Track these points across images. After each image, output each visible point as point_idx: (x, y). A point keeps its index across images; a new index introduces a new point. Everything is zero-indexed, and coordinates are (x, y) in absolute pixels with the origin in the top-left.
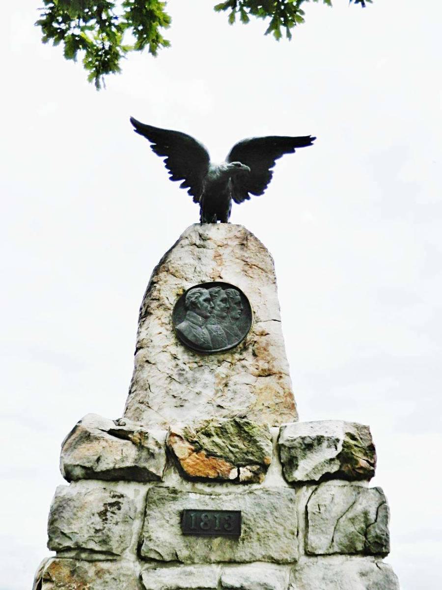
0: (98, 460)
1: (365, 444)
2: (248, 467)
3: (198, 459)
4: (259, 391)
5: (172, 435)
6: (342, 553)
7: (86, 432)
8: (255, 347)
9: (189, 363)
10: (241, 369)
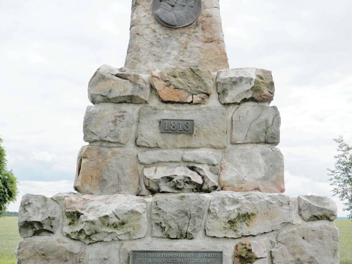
0: (110, 91)
1: (268, 82)
2: (198, 95)
3: (169, 90)
4: (205, 52)
5: (153, 76)
6: (251, 143)
7: (102, 75)
9: (163, 34)
10: (195, 38)
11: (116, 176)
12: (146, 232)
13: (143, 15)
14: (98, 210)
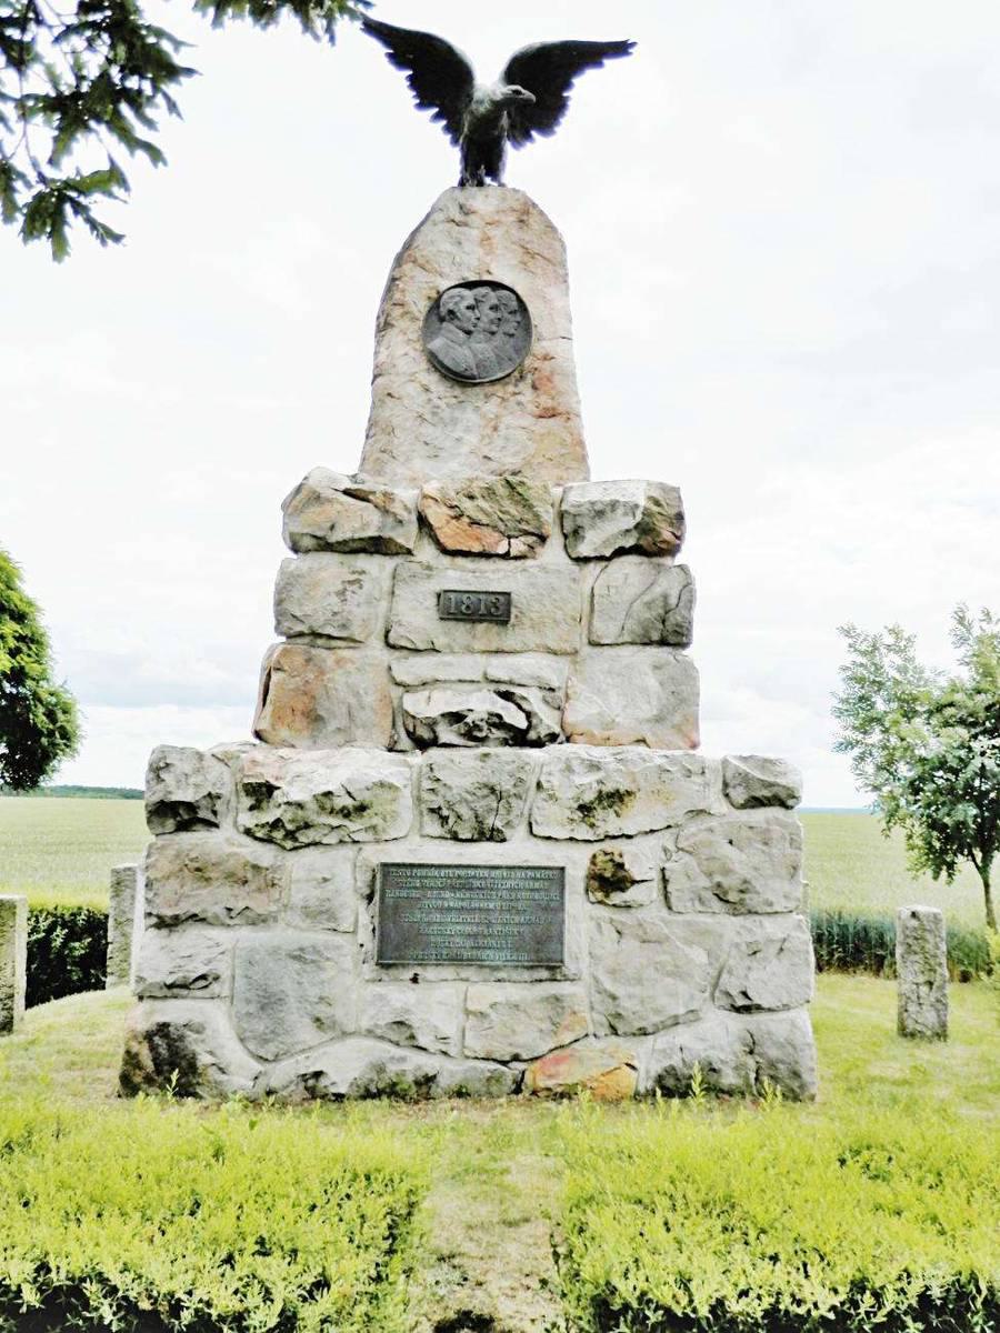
0: (332, 527)
1: (673, 512)
2: (522, 539)
4: (538, 438)
5: (425, 497)
6: (632, 643)
7: (315, 492)
8: (536, 376)
9: (446, 397)
10: (516, 407)
11: (344, 710)
12: (409, 826)
13: (403, 352)
14: (310, 781)
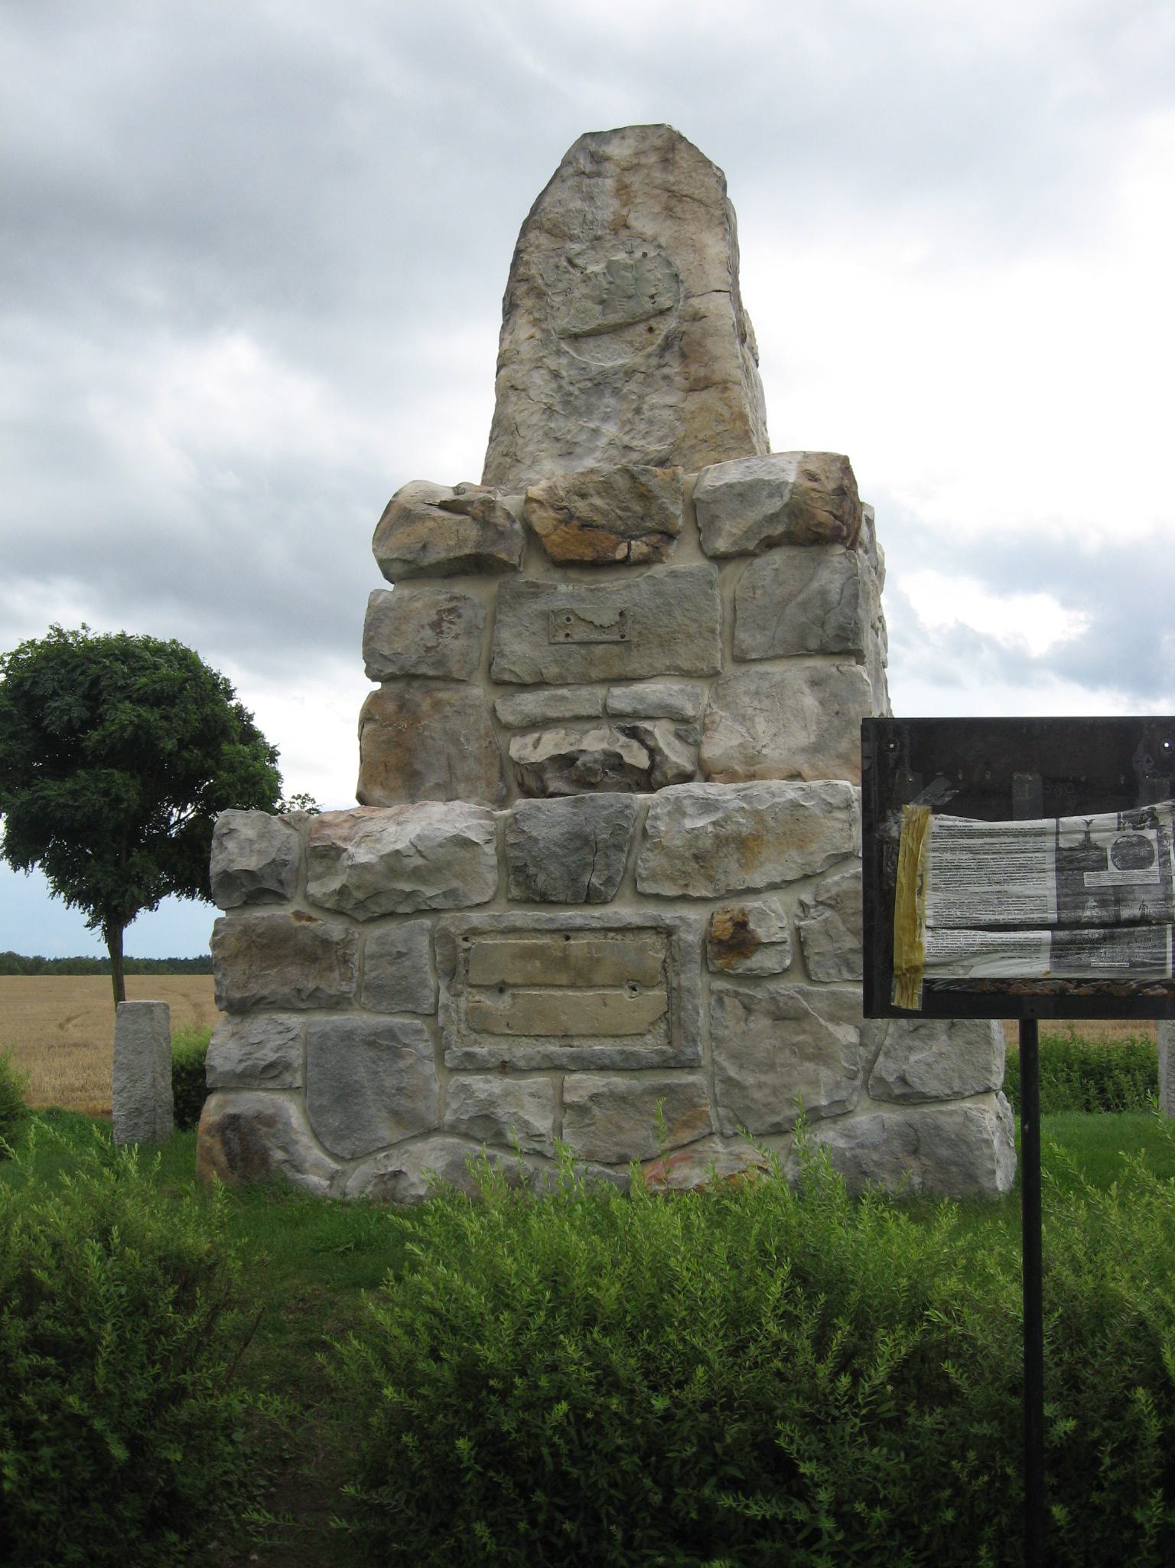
2: (644, 539)
3: (567, 533)
5: (529, 500)
8: (683, 341)
10: (661, 383)
11: (443, 761)
12: (494, 888)
13: (527, 336)
14: (378, 841)
